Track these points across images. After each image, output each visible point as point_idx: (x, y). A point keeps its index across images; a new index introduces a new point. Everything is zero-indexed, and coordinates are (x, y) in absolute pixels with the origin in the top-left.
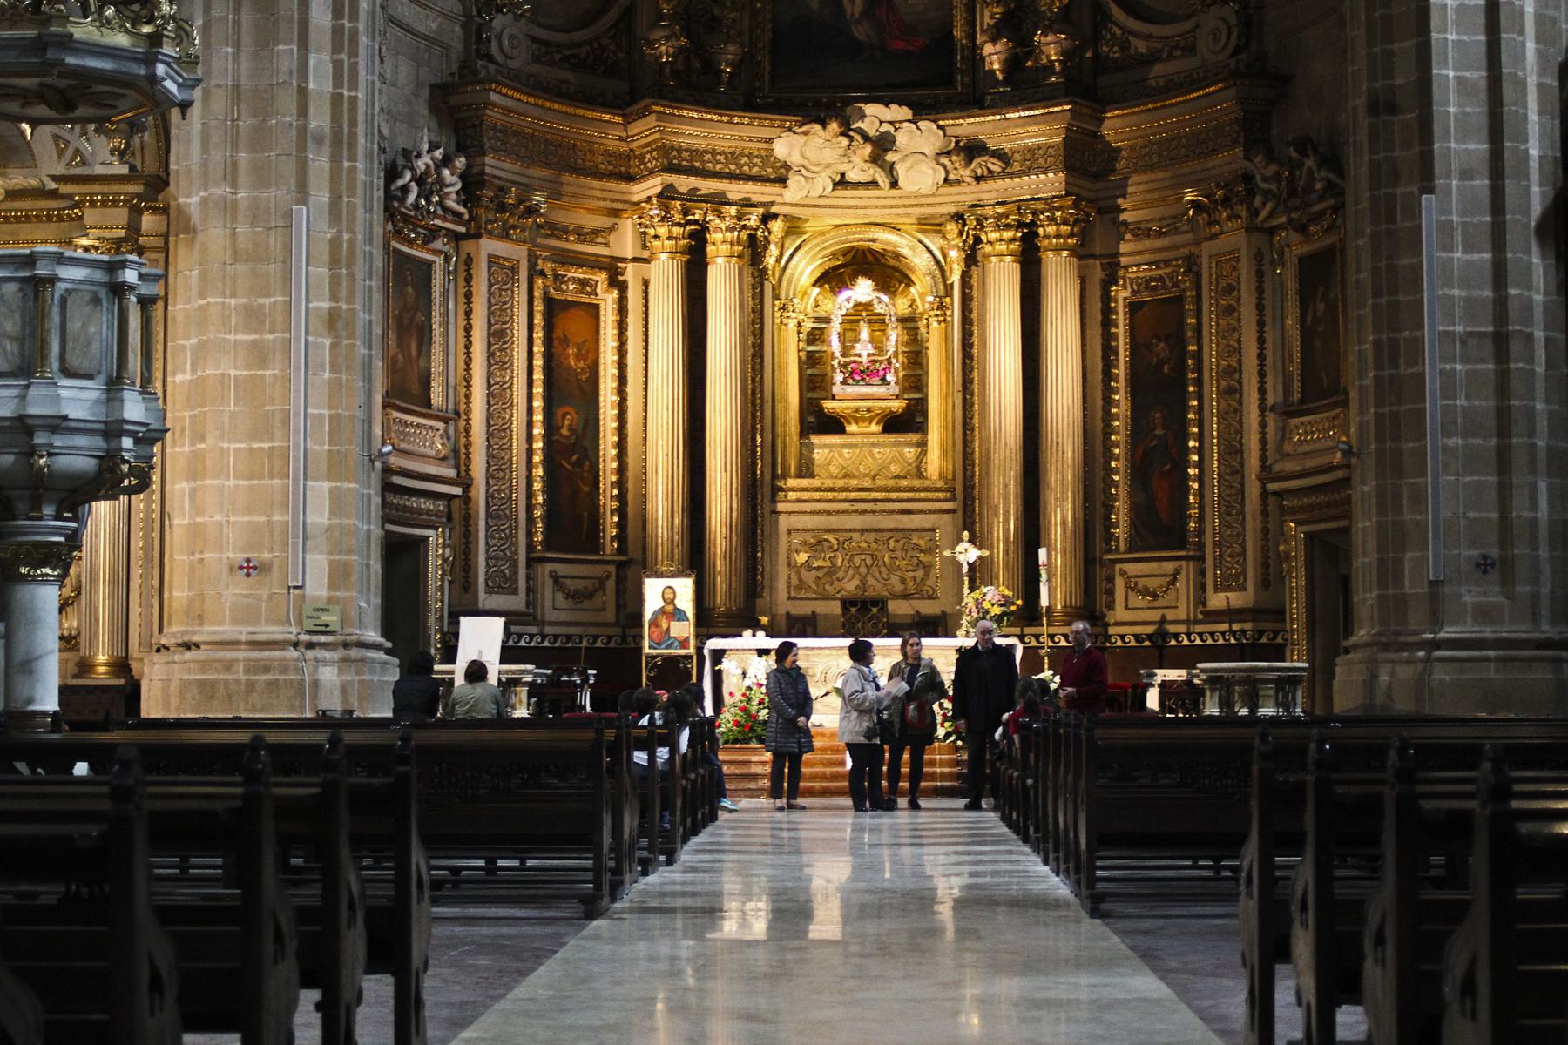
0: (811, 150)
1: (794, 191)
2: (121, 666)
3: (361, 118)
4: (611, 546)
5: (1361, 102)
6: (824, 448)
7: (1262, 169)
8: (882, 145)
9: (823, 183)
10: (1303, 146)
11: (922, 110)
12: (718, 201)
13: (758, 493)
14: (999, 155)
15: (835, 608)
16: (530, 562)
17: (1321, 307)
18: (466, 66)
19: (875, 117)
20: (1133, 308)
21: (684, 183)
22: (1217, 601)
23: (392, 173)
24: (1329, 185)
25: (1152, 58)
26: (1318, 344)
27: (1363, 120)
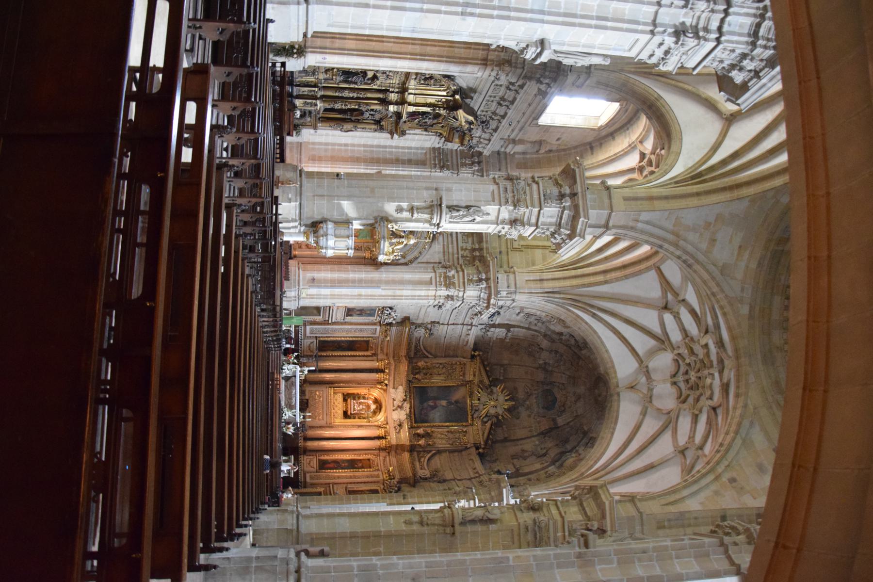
0: (398, 394)
1: (392, 390)
2: (295, 256)
3: (337, 291)
4: (320, 354)
6: (340, 398)
7: (395, 481)
8: (400, 407)
9: (394, 396)
11: (409, 416)
12: (389, 374)
13: (330, 383)
14: (399, 432)
15: (307, 397)
16: (316, 337)
18: (413, 324)
19: (407, 406)
20: (369, 460)
21: (393, 368)
22: (308, 476)
23: (391, 308)
25: (419, 461)
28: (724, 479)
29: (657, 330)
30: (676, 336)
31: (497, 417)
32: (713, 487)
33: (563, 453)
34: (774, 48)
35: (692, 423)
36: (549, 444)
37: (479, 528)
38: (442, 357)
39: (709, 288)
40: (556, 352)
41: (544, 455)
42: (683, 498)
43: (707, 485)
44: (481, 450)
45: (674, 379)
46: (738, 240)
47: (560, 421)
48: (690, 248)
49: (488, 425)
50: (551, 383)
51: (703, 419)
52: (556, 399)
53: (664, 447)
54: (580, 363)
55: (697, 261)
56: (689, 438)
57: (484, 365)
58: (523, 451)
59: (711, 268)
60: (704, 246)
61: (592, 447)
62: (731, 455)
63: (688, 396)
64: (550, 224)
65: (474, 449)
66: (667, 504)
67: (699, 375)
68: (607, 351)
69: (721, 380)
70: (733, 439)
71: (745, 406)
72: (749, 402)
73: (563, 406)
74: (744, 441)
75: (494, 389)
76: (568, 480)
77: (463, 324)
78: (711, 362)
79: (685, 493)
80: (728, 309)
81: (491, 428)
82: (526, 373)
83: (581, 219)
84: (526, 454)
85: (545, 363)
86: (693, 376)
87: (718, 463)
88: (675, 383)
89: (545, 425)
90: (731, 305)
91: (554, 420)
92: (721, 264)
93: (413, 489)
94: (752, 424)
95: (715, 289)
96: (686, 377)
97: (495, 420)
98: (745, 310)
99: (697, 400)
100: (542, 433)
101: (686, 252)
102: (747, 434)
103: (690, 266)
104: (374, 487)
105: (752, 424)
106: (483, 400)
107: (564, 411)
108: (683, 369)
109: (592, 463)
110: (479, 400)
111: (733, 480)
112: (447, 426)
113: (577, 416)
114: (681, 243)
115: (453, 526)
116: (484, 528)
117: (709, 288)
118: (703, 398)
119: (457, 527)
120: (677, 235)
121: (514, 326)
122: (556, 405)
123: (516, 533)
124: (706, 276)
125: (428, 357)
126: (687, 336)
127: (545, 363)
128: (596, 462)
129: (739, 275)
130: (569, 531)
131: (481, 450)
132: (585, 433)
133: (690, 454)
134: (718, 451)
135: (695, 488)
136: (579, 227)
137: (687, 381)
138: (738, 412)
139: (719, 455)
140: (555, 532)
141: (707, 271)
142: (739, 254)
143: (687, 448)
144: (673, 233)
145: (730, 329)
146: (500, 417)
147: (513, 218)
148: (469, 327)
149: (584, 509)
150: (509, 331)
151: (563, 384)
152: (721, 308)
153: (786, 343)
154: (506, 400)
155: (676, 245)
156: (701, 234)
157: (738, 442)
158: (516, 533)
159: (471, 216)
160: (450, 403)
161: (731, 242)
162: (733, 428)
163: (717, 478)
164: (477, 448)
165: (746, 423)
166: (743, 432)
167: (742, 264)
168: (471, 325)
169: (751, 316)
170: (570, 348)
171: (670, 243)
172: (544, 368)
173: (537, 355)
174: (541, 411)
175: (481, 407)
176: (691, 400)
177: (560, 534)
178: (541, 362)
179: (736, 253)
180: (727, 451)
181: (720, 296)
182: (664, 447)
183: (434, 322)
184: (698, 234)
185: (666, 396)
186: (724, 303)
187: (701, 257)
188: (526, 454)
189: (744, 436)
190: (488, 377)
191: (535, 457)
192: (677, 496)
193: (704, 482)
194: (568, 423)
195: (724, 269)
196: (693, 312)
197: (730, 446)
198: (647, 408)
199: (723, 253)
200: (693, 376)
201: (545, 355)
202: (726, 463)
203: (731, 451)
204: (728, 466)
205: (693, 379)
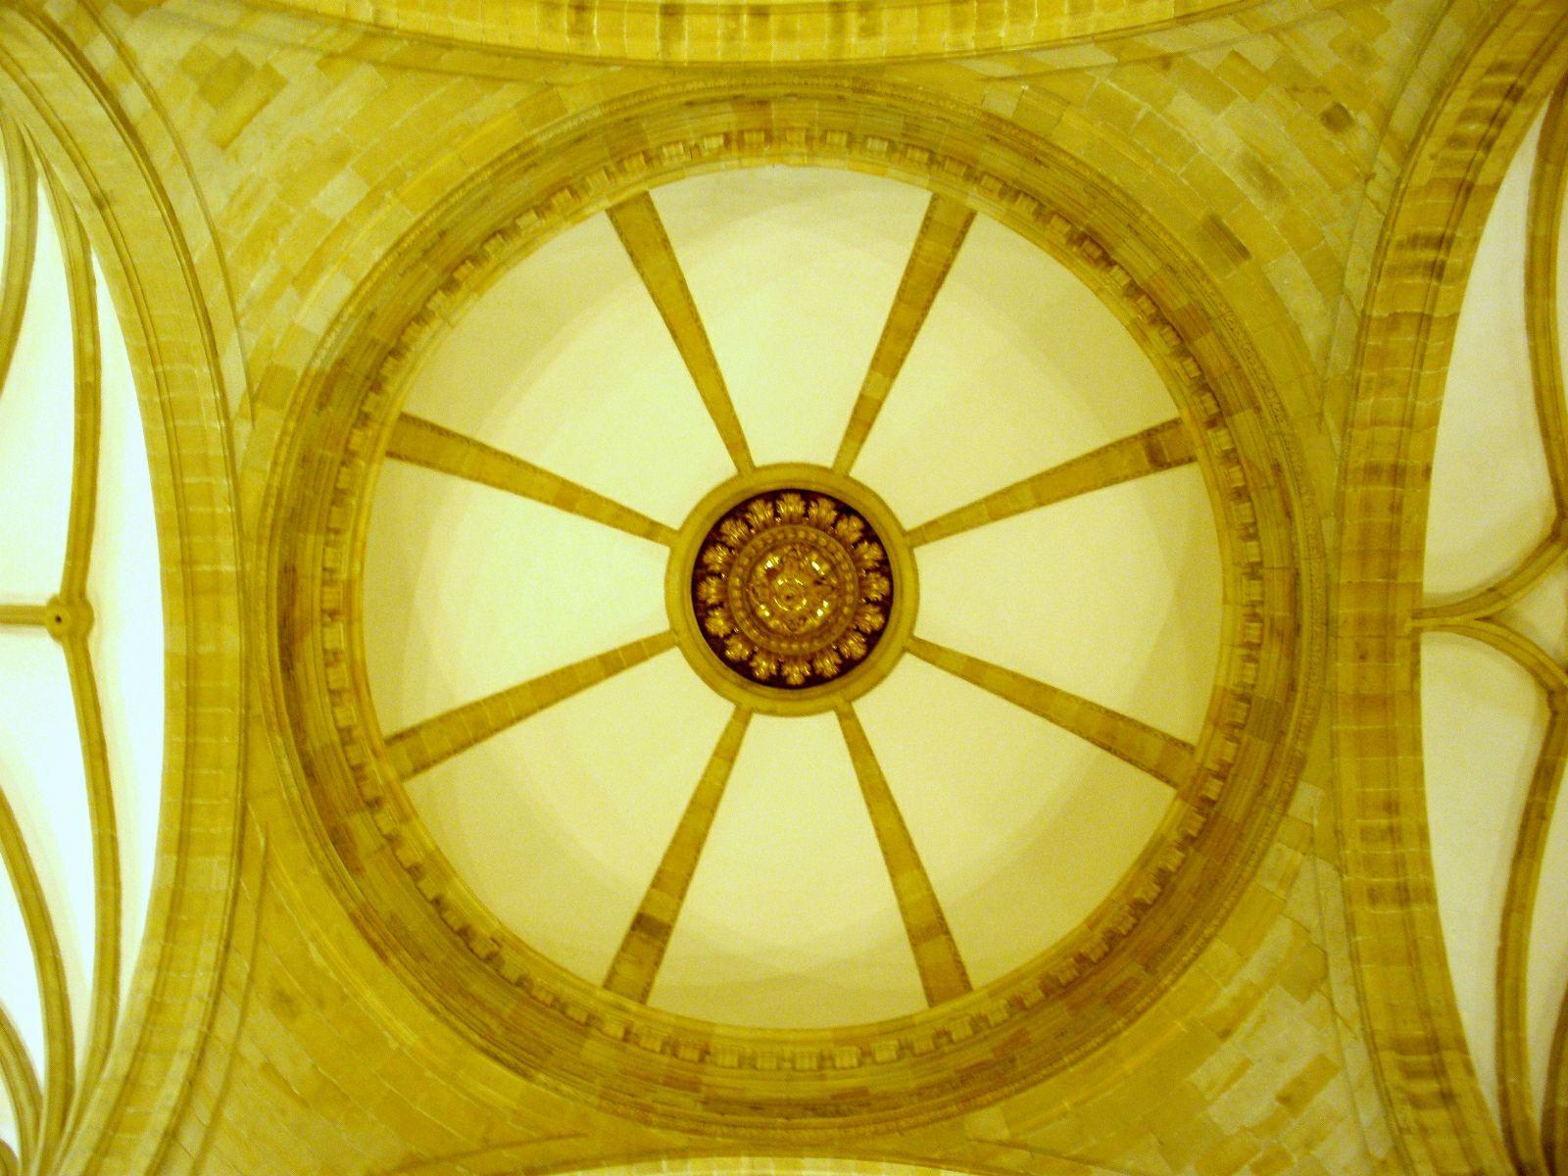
28: (1364, 119)
60: (1329, 1097)
72: (1336, 441)
92: (1317, 1000)
98: (1307, 798)
111: (1336, 120)
129: (1279, 936)
156: (1308, 1145)
167: (1252, 972)
169: (1299, 764)
179: (1246, 1026)
180: (1381, 247)
184: (1317, 1152)
187: (1356, 1057)
195: (1310, 982)
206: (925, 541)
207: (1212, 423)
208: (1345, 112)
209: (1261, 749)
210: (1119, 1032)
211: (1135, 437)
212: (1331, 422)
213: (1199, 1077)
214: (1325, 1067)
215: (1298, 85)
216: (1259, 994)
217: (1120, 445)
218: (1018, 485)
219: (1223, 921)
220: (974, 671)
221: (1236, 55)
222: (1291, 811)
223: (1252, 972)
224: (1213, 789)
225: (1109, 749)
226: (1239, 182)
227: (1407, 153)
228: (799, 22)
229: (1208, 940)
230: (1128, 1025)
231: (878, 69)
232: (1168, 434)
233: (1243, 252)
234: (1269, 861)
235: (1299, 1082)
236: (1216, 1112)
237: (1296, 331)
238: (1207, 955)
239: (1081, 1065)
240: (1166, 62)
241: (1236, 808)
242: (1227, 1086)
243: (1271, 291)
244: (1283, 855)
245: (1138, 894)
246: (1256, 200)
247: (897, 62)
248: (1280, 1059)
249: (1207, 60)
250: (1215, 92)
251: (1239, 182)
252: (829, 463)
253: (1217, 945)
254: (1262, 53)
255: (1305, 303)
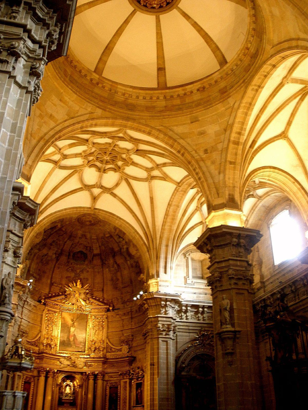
5: (149, 363)
10: (138, 368)
17: (139, 391)
20: (110, 388)
24: (142, 374)
26: (139, 396)
27: (149, 367)
28: (204, 156)
29: (66, 173)
30: (78, 161)
31: (88, 293)
32: (209, 163)
33: (121, 254)
34: (54, 12)
35: (137, 167)
36: (111, 261)
37: (236, 314)
38: (41, 326)
39: (77, 129)
40: (51, 244)
41: (118, 265)
42: (214, 183)
43: (207, 167)
44: (111, 308)
45: (102, 170)
46: (55, 99)
47: (96, 251)
48: (52, 133)
49: (92, 300)
50: (69, 253)
51: (136, 158)
52: (81, 252)
53: (141, 188)
54: (64, 230)
55: (60, 131)
56: (145, 170)
57: (51, 297)
58: (112, 280)
59: (67, 123)
61: (124, 234)
62: (189, 149)
63: (117, 164)
64: (20, 227)
65: (108, 313)
66: (218, 194)
67: (108, 153)
68: (65, 209)
69: (126, 141)
70: (179, 143)
71: (160, 131)
72: (157, 128)
73: (87, 247)
74: (181, 138)
75: (68, 293)
76: (147, 253)
77: (23, 307)
78: (106, 143)
79: (210, 181)
80: (94, 122)
81: (95, 299)
82: (59, 268)
83: (27, 203)
84: (114, 278)
85: (55, 254)
86: (106, 158)
87: (193, 157)
88: (105, 170)
89: (97, 261)
90: (93, 119)
91: (95, 255)
93: (137, 359)
94: (170, 130)
95: (80, 125)
96: (105, 162)
97: (89, 296)
98: (99, 112)
99: (124, 160)
100: (102, 265)
101: (53, 136)
102: (177, 134)
103: (60, 137)
104: (134, 386)
105: (170, 130)
106: (74, 301)
107: (90, 247)
108: (98, 164)
109: (138, 236)
110: (73, 304)
111: (206, 151)
112: (90, 329)
113: (97, 239)
114: (47, 137)
115: (235, 332)
116: (235, 311)
117: (77, 129)
118: (124, 156)
119: (237, 329)
120: (42, 138)
121: (29, 271)
122: (85, 252)
123: (238, 291)
124: (70, 129)
125: (40, 337)
126: (81, 154)
127: (55, 254)
128: (138, 233)
130: (237, 257)
131: (111, 308)
132: (111, 236)
133: (156, 173)
134: (183, 155)
135: (207, 174)
136: (30, 205)
137: (107, 162)
138: (162, 136)
139: (186, 155)
140: (237, 266)
141: (68, 127)
142: (64, 103)
143: (150, 175)
144: (39, 141)
145: (106, 125)
146: (87, 291)
147: (13, 255)
148: (26, 303)
149: (221, 245)
150: (32, 275)
151: (73, 244)
152: (91, 126)
153: (124, 95)
154: (76, 285)
155: (47, 142)
156: (45, 122)
157: (181, 141)
158: (238, 291)
159: (10, 288)
160: (73, 325)
161: (55, 105)
162: (171, 142)
163: (203, 160)
164: (108, 310)
165: (170, 133)
166: (175, 137)
167: (71, 103)
168: (25, 301)
170: (52, 234)
171: (45, 144)
172: (59, 256)
173: (49, 258)
174: (86, 263)
175: (79, 304)
176: (120, 163)
177: (238, 263)
178: (54, 256)
180: (186, 149)
181: (84, 124)
182: (141, 188)
183: (19, 329)
185: (110, 179)
186: (91, 122)
188: (114, 278)
189: (179, 137)
190: (59, 295)
191: (119, 274)
192: (212, 186)
193: (205, 169)
194: (100, 247)
196: (71, 146)
197: (183, 147)
198: (112, 192)
199: (60, 114)
200: (106, 158)
201: (51, 253)
202: (194, 152)
203: (187, 148)
204: (196, 151)
205: (108, 158)
206: (156, 19)
207: (165, 96)
208: (206, 154)
209: (106, 95)
210: (61, 80)
211: (164, 66)
212: (160, 128)
213: (54, 97)
214: (56, 121)
215: (214, 149)
216: (67, 105)
217: (164, 62)
218: (162, 39)
219: (79, 96)
220: (127, 22)
221: (221, 142)
222: (97, 108)
223: (71, 103)
224: (100, 85)
225: (106, 47)
226: (203, 129)
227: (197, 161)
228: (260, 81)
229: (76, 94)
230: (63, 81)
231: (246, 88)
232: (164, 74)
233: (192, 123)
234: (89, 104)
235: (54, 117)
236: (49, 103)
237: (177, 126)
238: (74, 94)
239: (56, 74)
240: (225, 130)
241: (96, 90)
242: (52, 103)
243: (184, 124)
244: (90, 108)
245: (83, 71)
246: (199, 130)
247: (245, 92)
248: (57, 112)
249: (222, 137)
250: (218, 134)
251: (203, 129)
252: (179, 6)
253: (75, 96)
254: (220, 146)
255: (180, 130)
